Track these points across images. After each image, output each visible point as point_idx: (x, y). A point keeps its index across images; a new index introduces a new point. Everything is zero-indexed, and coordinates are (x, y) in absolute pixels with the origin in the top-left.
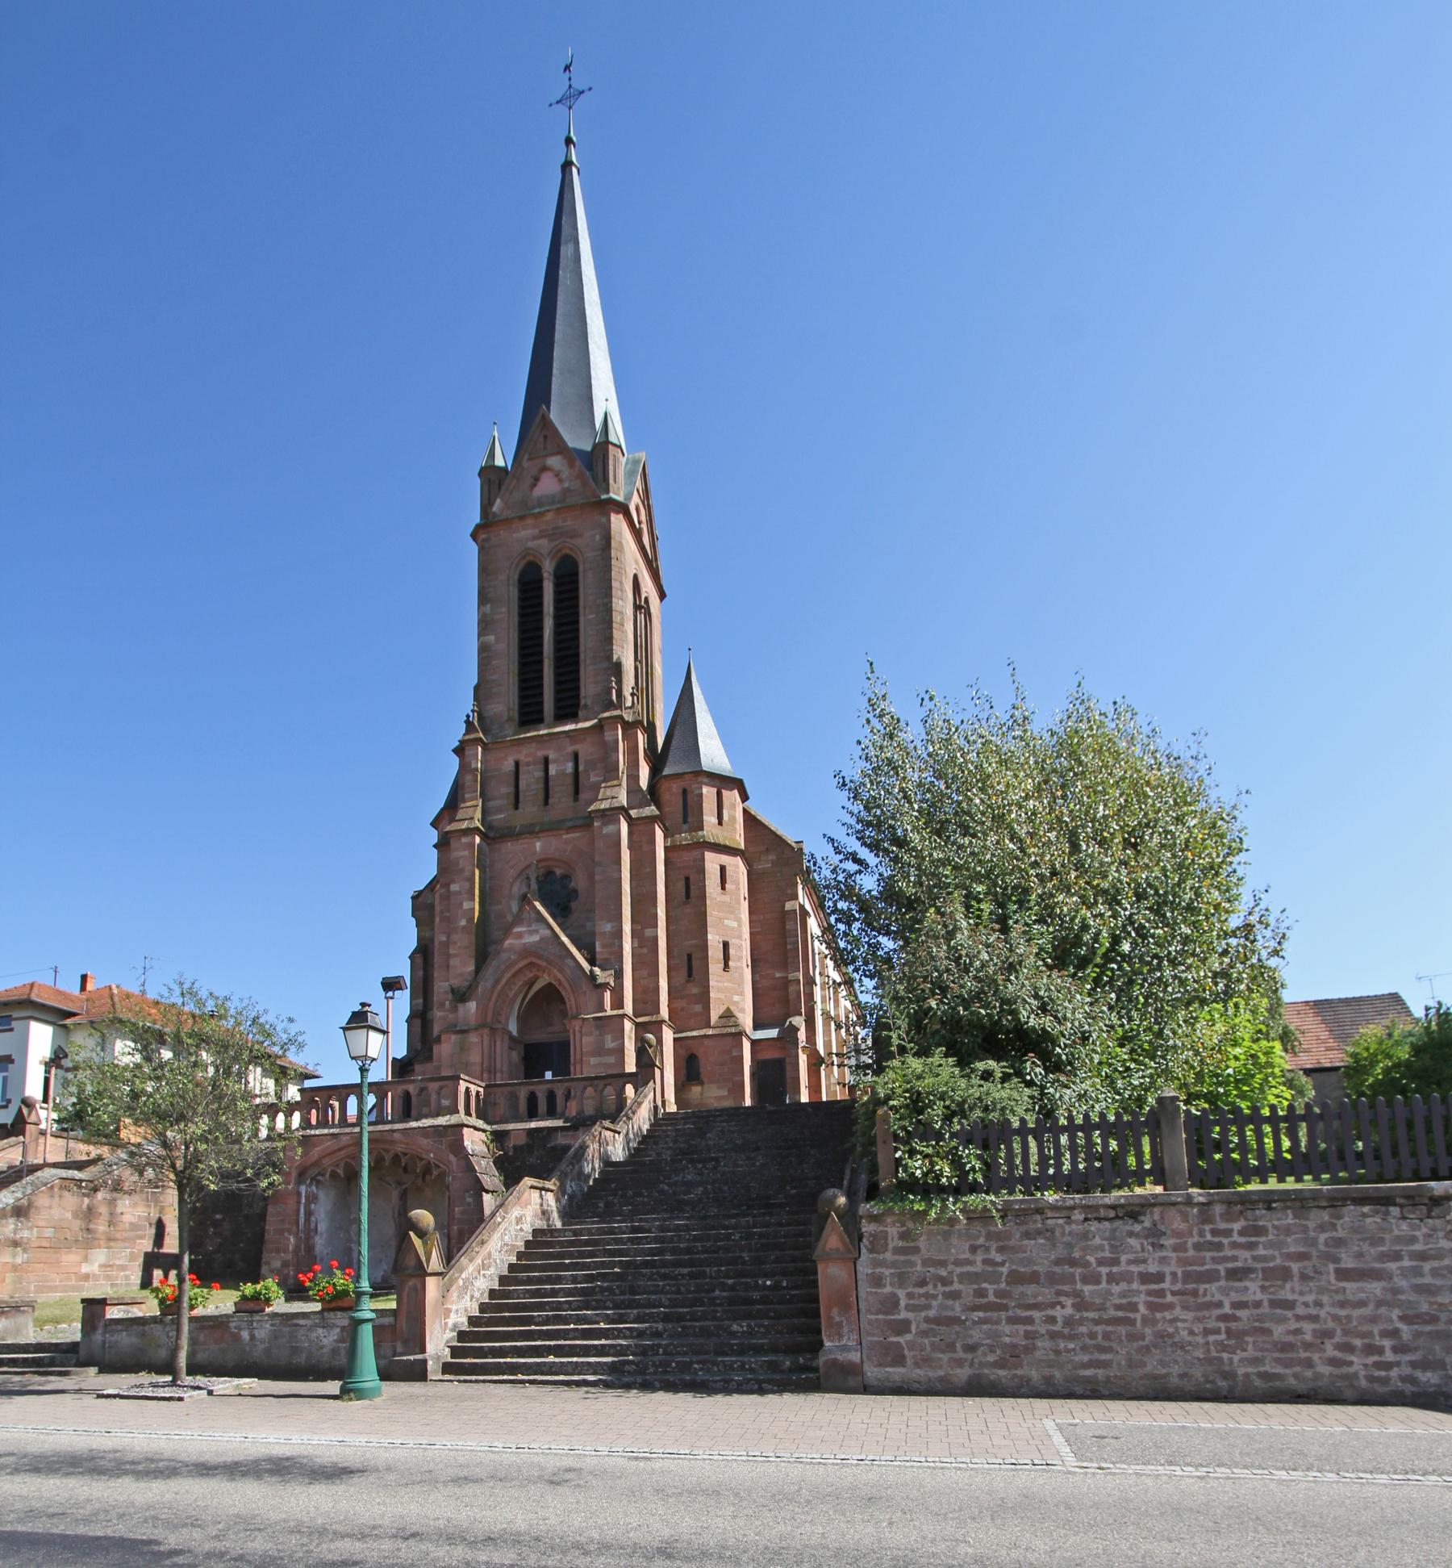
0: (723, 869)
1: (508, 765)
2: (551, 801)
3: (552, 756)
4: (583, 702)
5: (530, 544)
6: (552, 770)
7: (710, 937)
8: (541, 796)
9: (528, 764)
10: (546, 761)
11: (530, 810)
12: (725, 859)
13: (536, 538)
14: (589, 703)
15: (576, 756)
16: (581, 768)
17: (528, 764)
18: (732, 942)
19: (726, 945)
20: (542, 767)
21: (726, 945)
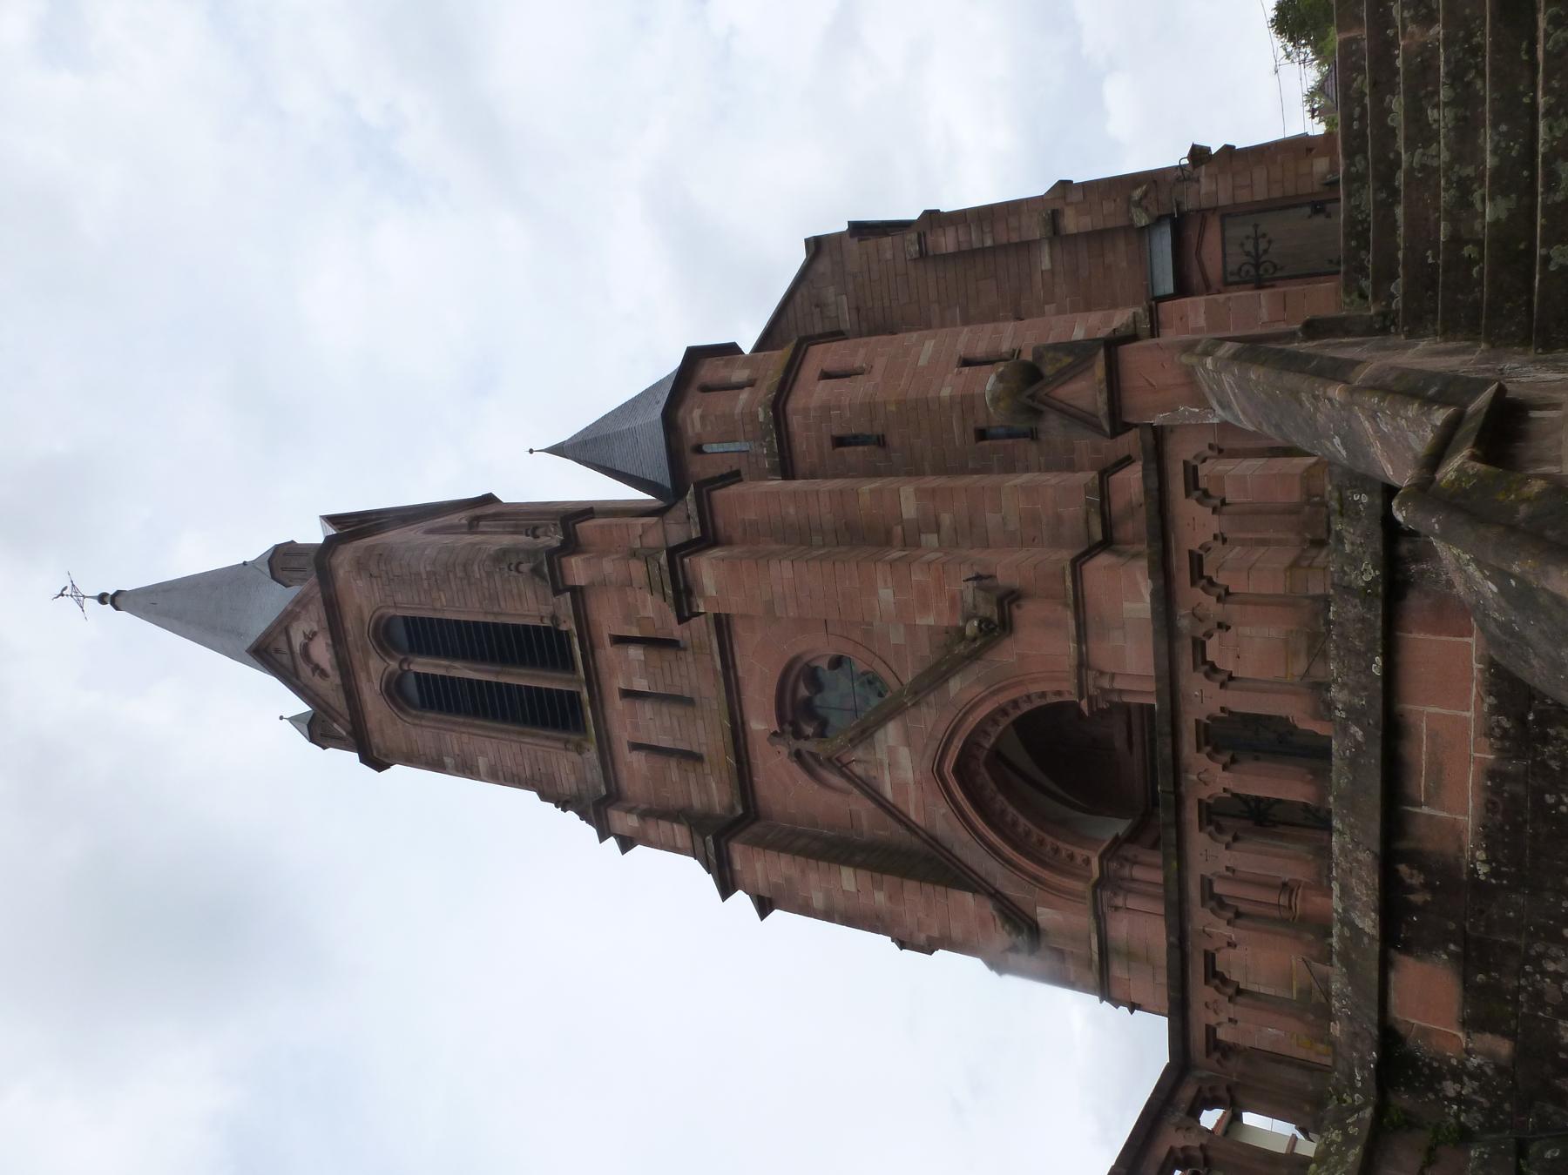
0: (826, 376)
1: (637, 760)
2: (687, 694)
3: (620, 683)
4: (547, 623)
5: (377, 687)
6: (641, 685)
7: (946, 392)
8: (678, 711)
9: (636, 727)
10: (628, 694)
11: (707, 735)
12: (810, 370)
13: (369, 680)
14: (546, 610)
15: (620, 640)
16: (635, 632)
17: (636, 727)
18: (961, 350)
19: (966, 362)
20: (638, 704)
21: (966, 362)
